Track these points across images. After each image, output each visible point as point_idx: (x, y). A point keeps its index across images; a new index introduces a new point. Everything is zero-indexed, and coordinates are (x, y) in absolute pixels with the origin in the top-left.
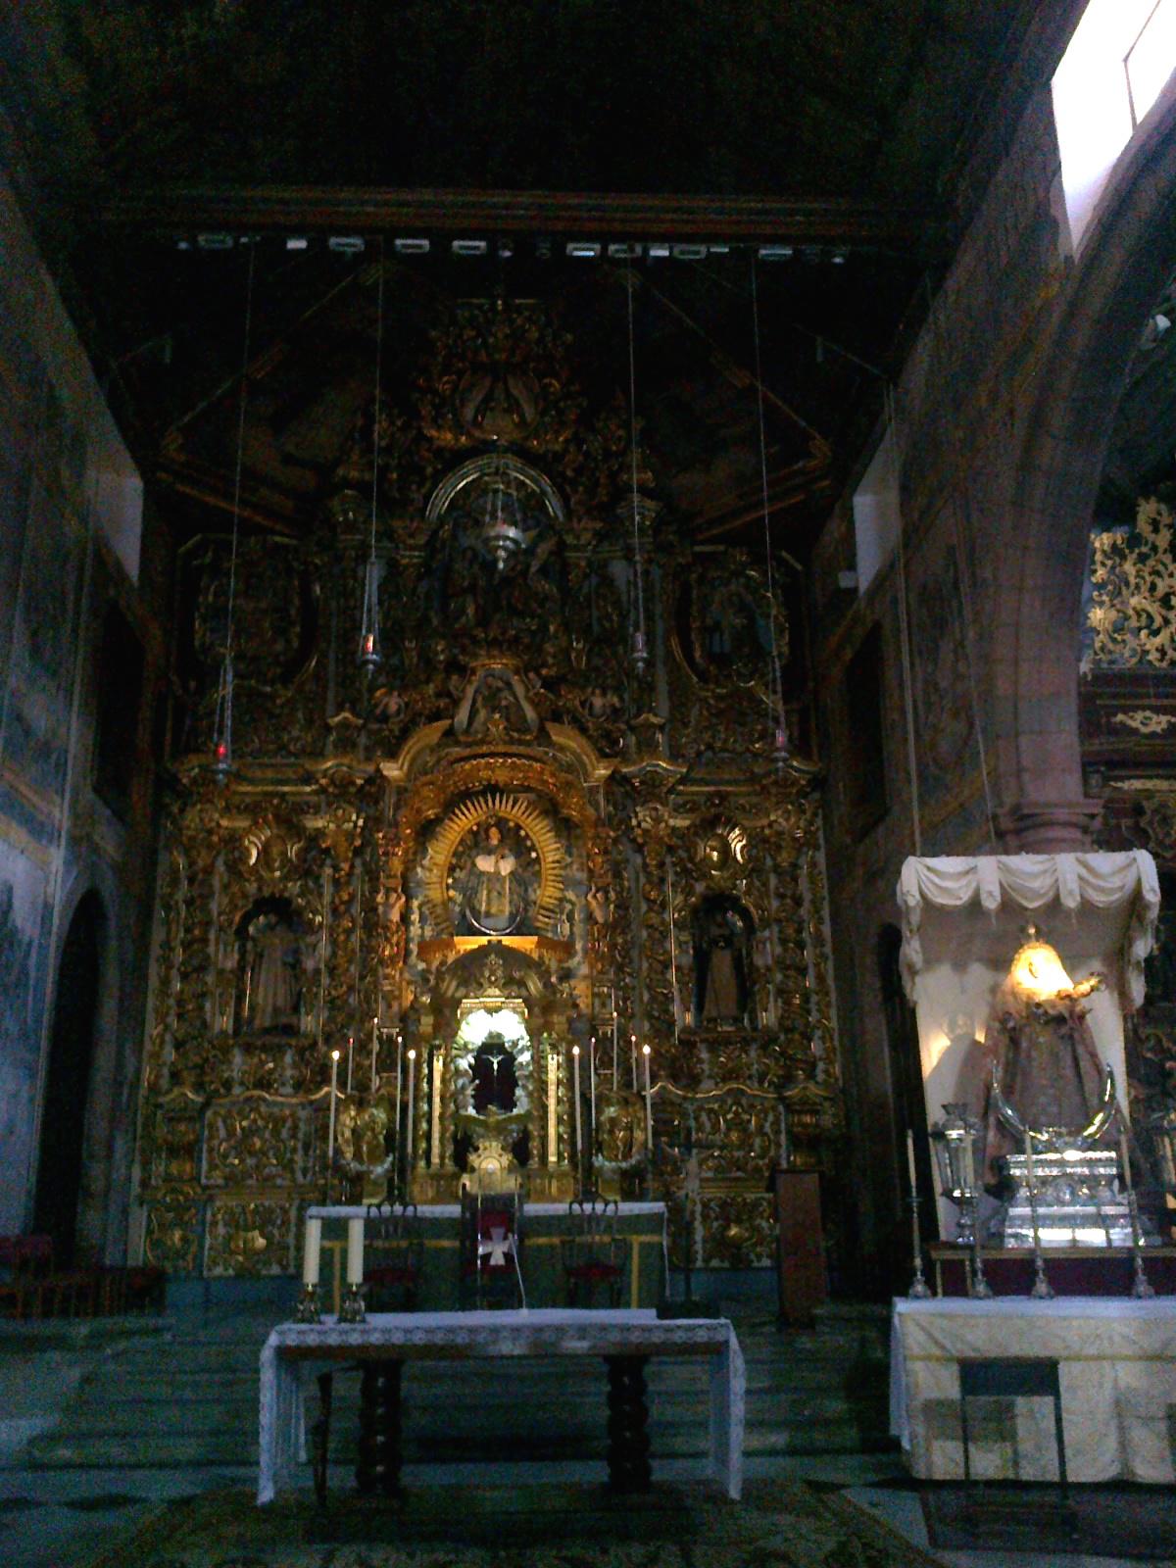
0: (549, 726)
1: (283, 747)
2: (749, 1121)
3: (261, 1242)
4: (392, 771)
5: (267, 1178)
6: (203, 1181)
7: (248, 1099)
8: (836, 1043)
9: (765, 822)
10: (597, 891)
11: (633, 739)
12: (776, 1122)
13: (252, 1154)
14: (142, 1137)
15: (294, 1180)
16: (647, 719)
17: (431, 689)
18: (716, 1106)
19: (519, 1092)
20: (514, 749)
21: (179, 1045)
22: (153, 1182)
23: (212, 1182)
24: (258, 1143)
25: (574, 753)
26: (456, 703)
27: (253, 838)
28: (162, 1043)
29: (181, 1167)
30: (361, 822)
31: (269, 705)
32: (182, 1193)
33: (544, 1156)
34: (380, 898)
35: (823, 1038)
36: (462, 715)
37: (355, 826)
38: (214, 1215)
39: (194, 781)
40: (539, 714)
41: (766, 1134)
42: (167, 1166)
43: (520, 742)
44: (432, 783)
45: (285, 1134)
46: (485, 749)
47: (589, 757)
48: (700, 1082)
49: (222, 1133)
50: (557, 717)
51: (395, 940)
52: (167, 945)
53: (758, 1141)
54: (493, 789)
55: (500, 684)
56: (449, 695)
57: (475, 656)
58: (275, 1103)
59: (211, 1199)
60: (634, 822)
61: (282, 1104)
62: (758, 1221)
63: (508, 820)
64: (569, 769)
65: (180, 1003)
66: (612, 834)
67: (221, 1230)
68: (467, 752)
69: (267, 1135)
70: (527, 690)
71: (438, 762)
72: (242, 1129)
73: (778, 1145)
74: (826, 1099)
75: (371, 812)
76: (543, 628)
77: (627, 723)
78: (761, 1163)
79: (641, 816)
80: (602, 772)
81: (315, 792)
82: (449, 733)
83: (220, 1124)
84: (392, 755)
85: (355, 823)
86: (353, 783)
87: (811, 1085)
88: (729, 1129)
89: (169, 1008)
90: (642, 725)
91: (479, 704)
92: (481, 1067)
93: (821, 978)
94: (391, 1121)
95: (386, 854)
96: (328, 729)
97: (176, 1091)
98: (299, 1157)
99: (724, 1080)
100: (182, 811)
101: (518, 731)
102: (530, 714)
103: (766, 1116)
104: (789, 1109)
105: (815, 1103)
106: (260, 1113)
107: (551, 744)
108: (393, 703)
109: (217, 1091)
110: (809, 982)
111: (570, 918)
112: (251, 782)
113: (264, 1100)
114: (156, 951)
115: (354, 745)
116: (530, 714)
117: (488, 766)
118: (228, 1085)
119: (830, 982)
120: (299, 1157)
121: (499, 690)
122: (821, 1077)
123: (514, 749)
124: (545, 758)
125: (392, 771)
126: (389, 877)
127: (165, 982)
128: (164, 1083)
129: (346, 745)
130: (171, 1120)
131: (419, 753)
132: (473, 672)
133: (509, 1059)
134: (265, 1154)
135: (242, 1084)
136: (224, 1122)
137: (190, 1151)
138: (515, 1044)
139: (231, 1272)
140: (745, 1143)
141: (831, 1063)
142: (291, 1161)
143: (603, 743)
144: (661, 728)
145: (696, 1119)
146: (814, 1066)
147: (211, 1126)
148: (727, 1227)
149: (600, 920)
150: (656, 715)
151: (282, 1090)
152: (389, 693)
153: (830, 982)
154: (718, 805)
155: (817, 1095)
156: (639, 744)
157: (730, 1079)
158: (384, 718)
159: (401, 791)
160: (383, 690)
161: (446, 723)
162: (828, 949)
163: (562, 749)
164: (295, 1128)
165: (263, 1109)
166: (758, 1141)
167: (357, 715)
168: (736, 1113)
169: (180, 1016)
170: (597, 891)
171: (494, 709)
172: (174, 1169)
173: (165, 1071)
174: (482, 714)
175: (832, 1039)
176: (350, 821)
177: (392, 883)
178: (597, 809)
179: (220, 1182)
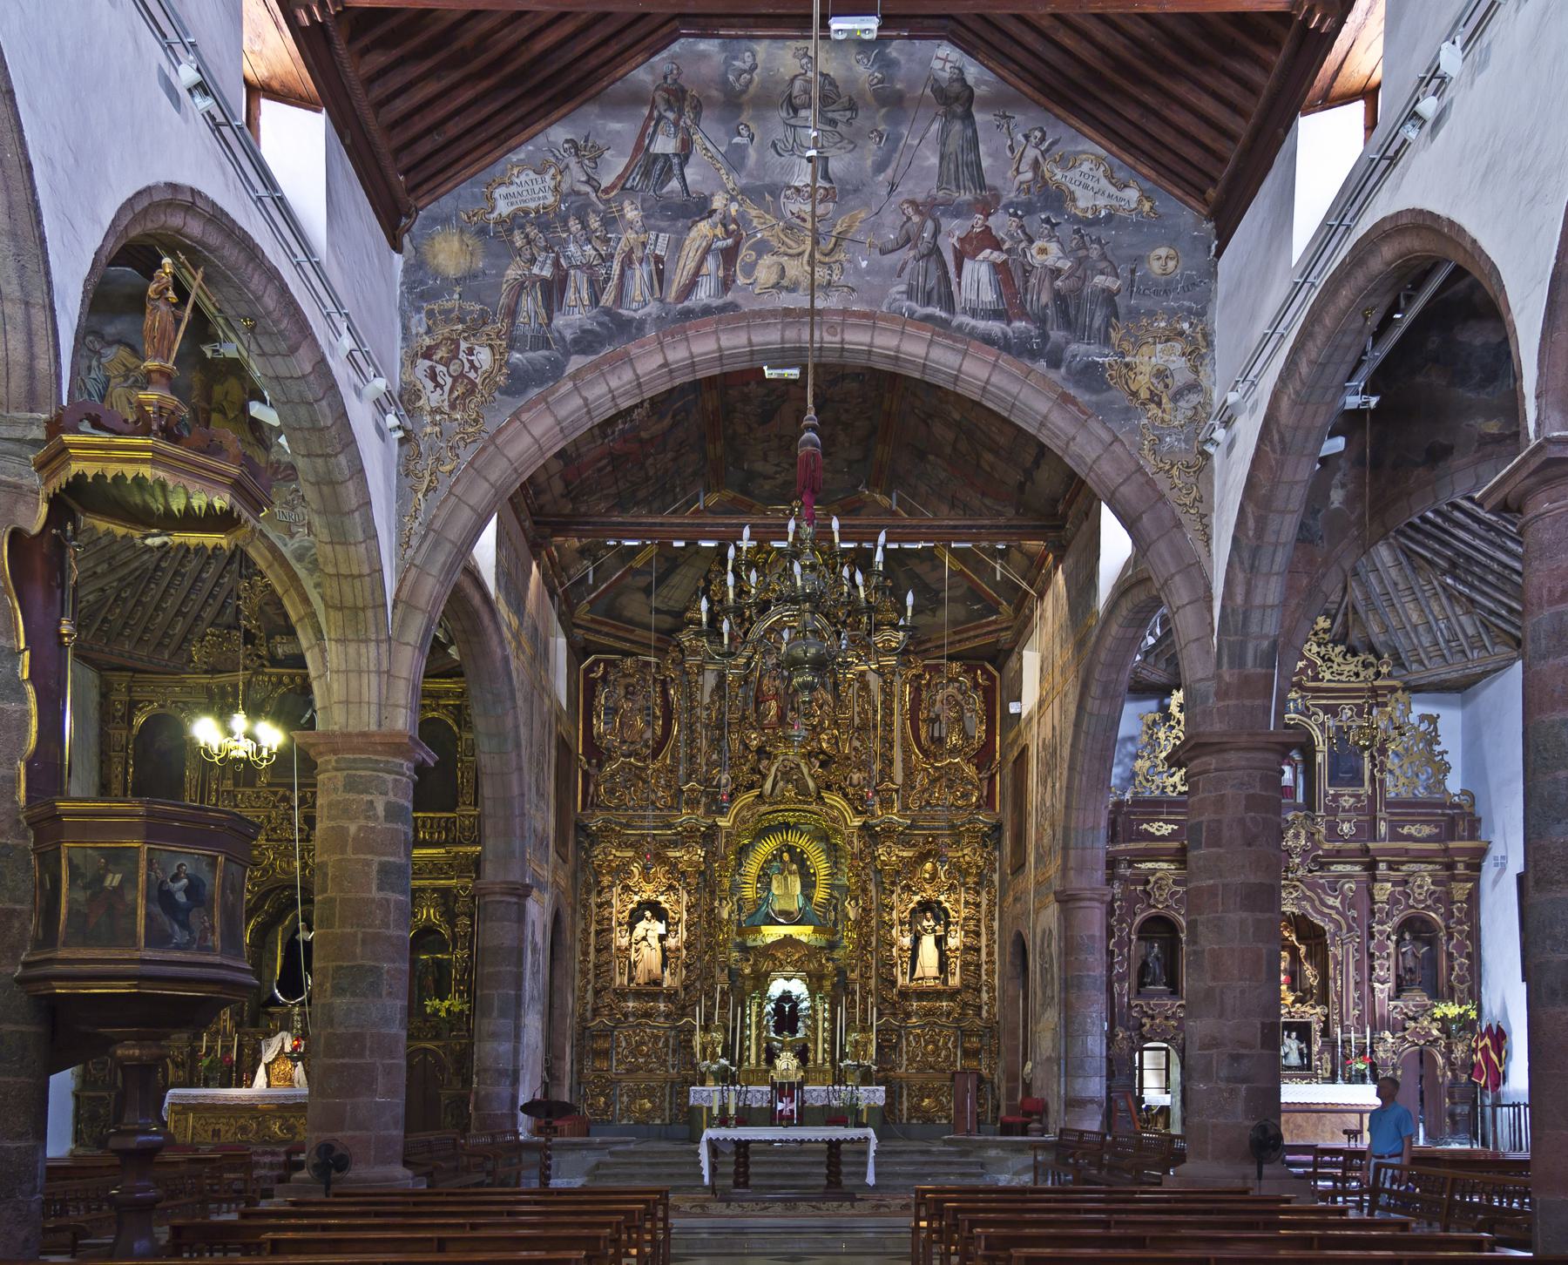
3: (648, 1105)
4: (723, 822)
5: (651, 1071)
7: (638, 1025)
9: (960, 854)
11: (877, 799)
15: (667, 1071)
19: (800, 1024)
20: (800, 806)
21: (597, 993)
25: (838, 809)
26: (764, 777)
33: (815, 1060)
34: (716, 904)
35: (988, 992)
36: (768, 785)
39: (599, 829)
40: (816, 784)
43: (806, 803)
46: (782, 807)
47: (849, 814)
49: (624, 1044)
50: (828, 788)
52: (586, 931)
53: (943, 1053)
56: (760, 772)
58: (655, 1027)
59: (620, 1081)
64: (834, 820)
67: (625, 1099)
68: (771, 809)
70: (810, 770)
73: (956, 1054)
76: (821, 722)
80: (857, 822)
81: (674, 834)
82: (760, 796)
83: (622, 1038)
84: (722, 812)
86: (699, 830)
87: (978, 1021)
88: (926, 1046)
92: (778, 1010)
93: (990, 954)
94: (726, 1039)
95: (720, 876)
96: (682, 792)
99: (925, 1015)
100: (591, 845)
102: (811, 784)
107: (825, 804)
110: (984, 957)
113: (647, 1024)
114: (579, 935)
115: (699, 803)
116: (811, 784)
118: (626, 1015)
121: (791, 768)
122: (984, 1014)
123: (800, 806)
125: (723, 822)
127: (586, 953)
128: (589, 1014)
129: (693, 803)
131: (741, 809)
132: (776, 758)
133: (795, 1006)
135: (634, 1014)
137: (605, 1054)
138: (798, 997)
140: (936, 1052)
141: (993, 1006)
142: (665, 1061)
143: (857, 803)
144: (897, 791)
145: (907, 1039)
146: (980, 1008)
156: (881, 804)
159: (729, 835)
161: (756, 792)
162: (996, 936)
163: (832, 807)
164: (667, 1040)
166: (943, 1053)
169: (597, 976)
171: (788, 782)
173: (589, 1007)
175: (994, 991)
177: (723, 895)
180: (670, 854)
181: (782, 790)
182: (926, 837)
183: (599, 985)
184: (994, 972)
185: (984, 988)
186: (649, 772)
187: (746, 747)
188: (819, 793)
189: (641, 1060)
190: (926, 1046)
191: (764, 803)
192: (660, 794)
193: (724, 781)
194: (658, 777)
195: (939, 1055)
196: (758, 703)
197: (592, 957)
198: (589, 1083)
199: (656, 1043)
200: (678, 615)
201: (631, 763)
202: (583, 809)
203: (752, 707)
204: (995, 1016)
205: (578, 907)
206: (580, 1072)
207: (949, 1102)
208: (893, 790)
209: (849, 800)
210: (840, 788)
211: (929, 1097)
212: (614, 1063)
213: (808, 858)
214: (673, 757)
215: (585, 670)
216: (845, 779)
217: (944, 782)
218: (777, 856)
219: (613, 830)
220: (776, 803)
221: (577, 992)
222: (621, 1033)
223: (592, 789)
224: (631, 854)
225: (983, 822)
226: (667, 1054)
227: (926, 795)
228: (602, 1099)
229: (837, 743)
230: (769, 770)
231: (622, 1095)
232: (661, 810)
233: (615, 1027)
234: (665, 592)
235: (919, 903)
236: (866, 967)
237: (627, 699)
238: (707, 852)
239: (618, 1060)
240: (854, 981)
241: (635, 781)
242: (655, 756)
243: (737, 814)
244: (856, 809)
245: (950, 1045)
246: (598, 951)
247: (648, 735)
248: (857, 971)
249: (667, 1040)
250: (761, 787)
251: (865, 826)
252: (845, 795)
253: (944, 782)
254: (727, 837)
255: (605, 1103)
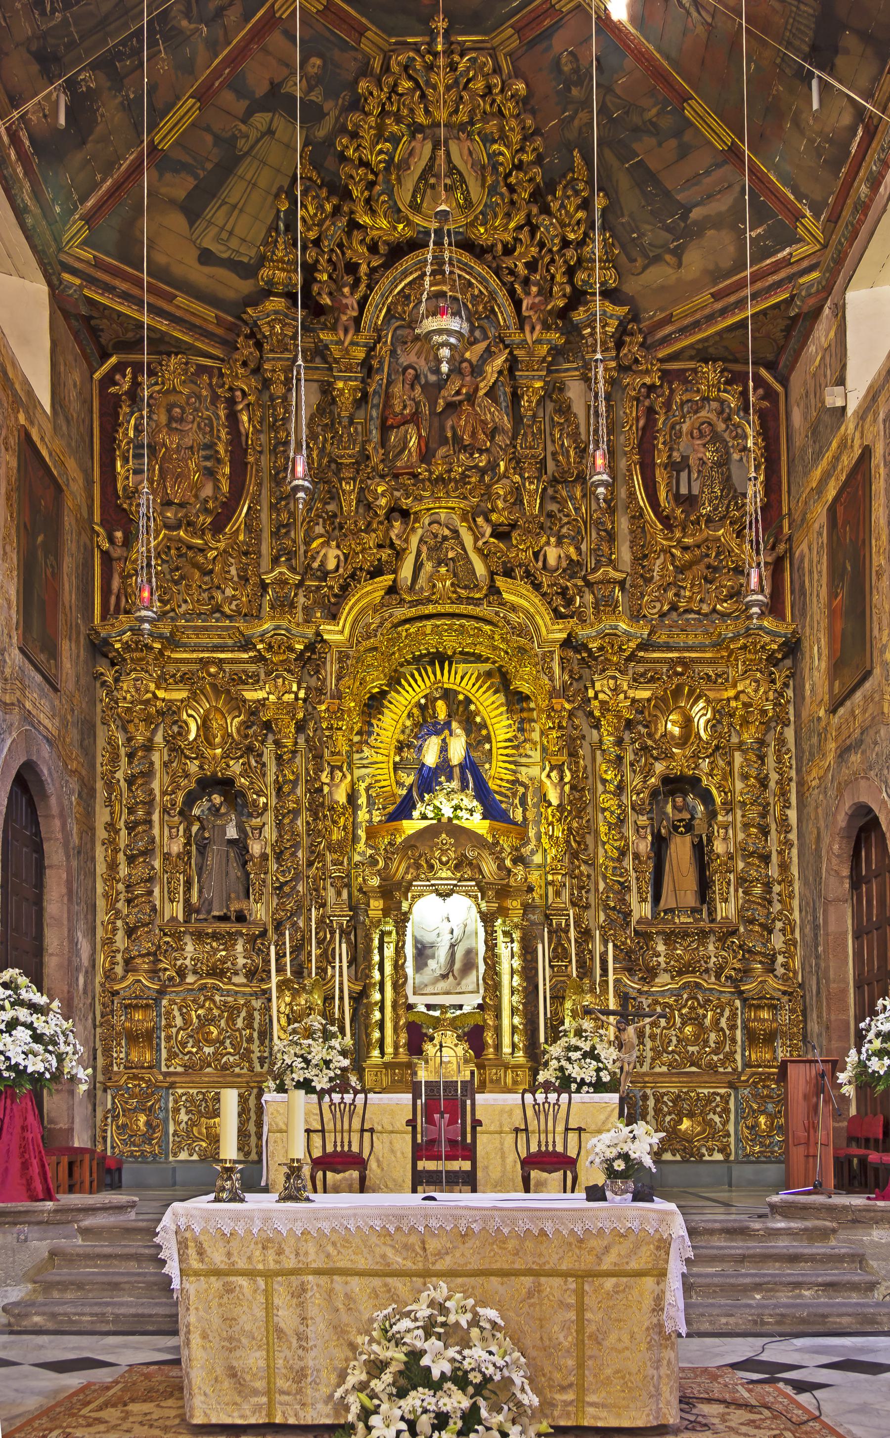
0: (501, 582)
1: (217, 609)
2: (705, 1016)
5: (225, 1067)
6: (164, 1069)
7: (203, 988)
8: (797, 935)
9: (731, 693)
10: (551, 770)
11: (589, 598)
12: (733, 1016)
13: (210, 1042)
14: (101, 1025)
15: (251, 1069)
16: (606, 573)
17: (371, 540)
18: (671, 1001)
20: (462, 609)
21: (130, 932)
22: (115, 1068)
23: (172, 1069)
24: (215, 1032)
25: (526, 612)
26: (399, 554)
27: (190, 712)
28: (115, 930)
29: (141, 1055)
30: (302, 694)
31: (201, 559)
32: (142, 1079)
33: (498, 1047)
34: (325, 777)
36: (406, 571)
37: (297, 698)
38: (176, 1102)
39: (127, 647)
40: (488, 567)
41: (722, 1029)
42: (127, 1054)
43: (470, 601)
44: (375, 649)
45: (240, 1023)
46: (430, 609)
48: (656, 975)
49: (179, 1021)
50: (508, 573)
51: (342, 823)
52: (111, 827)
54: (440, 659)
55: (447, 532)
56: (392, 545)
57: (419, 499)
58: (228, 993)
59: (172, 1085)
60: (591, 693)
61: (236, 992)
62: (711, 1116)
63: (457, 693)
64: (520, 631)
65: (129, 887)
66: (568, 706)
67: (183, 1117)
68: (413, 612)
69: (223, 1023)
70: (476, 539)
71: (381, 625)
72: (198, 1017)
73: (733, 1040)
74: (784, 993)
75: (313, 682)
76: (492, 466)
77: (584, 579)
78: (715, 1058)
79: (598, 686)
81: (252, 660)
82: (392, 590)
83: (176, 1013)
84: (334, 617)
85: (296, 694)
87: (771, 981)
88: (684, 1024)
89: (118, 893)
90: (601, 582)
91: (424, 555)
93: (784, 867)
95: (330, 728)
96: (264, 586)
97: (131, 978)
98: (255, 1047)
99: (680, 973)
100: (117, 680)
101: (465, 587)
102: (480, 569)
103: (723, 1011)
104: (744, 1001)
105: (772, 998)
106: (214, 1002)
107: (503, 604)
108: (332, 557)
109: (171, 979)
110: (774, 871)
111: (523, 802)
112: (185, 647)
113: (218, 989)
114: (102, 834)
115: (292, 605)
116: (480, 569)
117: (436, 629)
118: (181, 973)
119: (795, 870)
120: (255, 1047)
121: (445, 538)
122: (780, 971)
123: (462, 609)
124: (496, 619)
126: (333, 754)
127: (113, 866)
128: (119, 970)
129: (284, 605)
130: (127, 1007)
131: (362, 611)
132: (416, 520)
134: (222, 1043)
135: (195, 972)
136: (180, 1010)
137: (148, 1037)
139: (195, 1157)
140: (700, 1038)
141: (792, 956)
142: (249, 1051)
143: (558, 601)
144: (622, 584)
147: (168, 1013)
148: (680, 1122)
149: (555, 802)
150: (615, 569)
151: (236, 980)
152: (326, 544)
153: (795, 870)
154: (681, 674)
155: (774, 989)
156: (596, 606)
157: (688, 972)
158: (324, 574)
159: (343, 657)
160: (321, 540)
162: (793, 836)
163: (514, 608)
164: (250, 1017)
165: (217, 998)
166: (713, 1036)
167: (292, 569)
168: (692, 1008)
169: (129, 901)
170: (551, 770)
172: (134, 1057)
173: (119, 957)
174: (428, 567)
175: (793, 932)
176: (290, 692)
177: (336, 761)
178: (551, 679)
179: (180, 1069)
180: (249, 695)
181: (430, 579)
182: (672, 662)
183: (131, 920)
184: (791, 896)
185: (779, 925)
186: (211, 554)
187: (369, 507)
188: (492, 580)
189: (208, 1050)
190: (684, 1024)
191: (402, 601)
192: (229, 592)
193: (331, 565)
194: (226, 564)
195: (706, 1042)
196: (385, 429)
197: (123, 870)
198: (120, 1088)
199: (231, 1020)
200: (248, 271)
201: (180, 540)
202: (103, 618)
203: (375, 434)
204: (795, 973)
205: (99, 785)
206: (107, 1069)
207: (725, 1123)
208: (615, 582)
209: (544, 595)
210: (528, 574)
211: (691, 1115)
212: (164, 1055)
213: (477, 713)
214: (249, 528)
215: (101, 381)
216: (537, 561)
217: (700, 569)
218: (425, 708)
219: (150, 648)
220: (418, 603)
221: (100, 933)
222: (172, 1002)
223: (116, 583)
224: (184, 695)
225: (769, 633)
226: (250, 1040)
227: (670, 594)
228: (143, 1119)
229: (519, 501)
230: (406, 541)
231: (177, 1110)
232: (229, 617)
233: (161, 993)
234: (220, 217)
235: (666, 780)
236: (581, 888)
237: (171, 430)
238: (308, 689)
239: (169, 1050)
240: (561, 912)
241: (188, 569)
242: (218, 528)
243: (355, 621)
244: (555, 610)
245: (723, 1023)
246: (131, 860)
247: (208, 491)
248: (566, 895)
249: (250, 1017)
250: (395, 572)
251: (567, 643)
252: (537, 587)
253: (700, 569)
254: (340, 660)
255: (148, 1124)
